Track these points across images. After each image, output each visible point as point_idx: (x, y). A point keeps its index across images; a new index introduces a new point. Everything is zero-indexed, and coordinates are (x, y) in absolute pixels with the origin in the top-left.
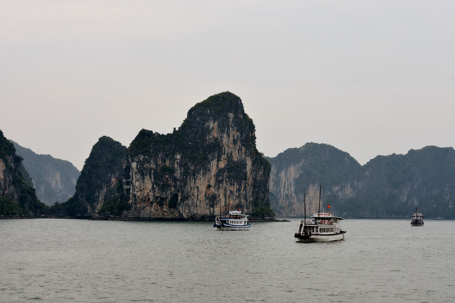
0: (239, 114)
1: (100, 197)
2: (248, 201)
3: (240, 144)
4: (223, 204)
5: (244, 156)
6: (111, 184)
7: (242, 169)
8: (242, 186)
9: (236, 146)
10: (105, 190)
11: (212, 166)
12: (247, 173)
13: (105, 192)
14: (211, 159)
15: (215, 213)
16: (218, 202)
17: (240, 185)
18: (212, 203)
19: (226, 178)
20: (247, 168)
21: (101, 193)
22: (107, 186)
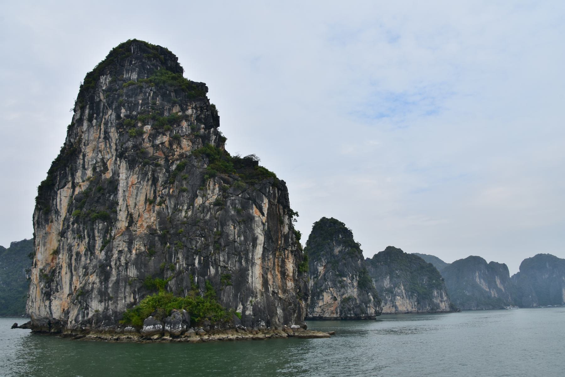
0: (125, 73)
2: (113, 278)
4: (66, 290)
6: (319, 274)
7: (108, 195)
8: (97, 238)
9: (110, 145)
11: (61, 201)
13: (312, 285)
16: (59, 286)
18: (49, 289)
19: (73, 224)
20: (119, 190)
22: (314, 278)
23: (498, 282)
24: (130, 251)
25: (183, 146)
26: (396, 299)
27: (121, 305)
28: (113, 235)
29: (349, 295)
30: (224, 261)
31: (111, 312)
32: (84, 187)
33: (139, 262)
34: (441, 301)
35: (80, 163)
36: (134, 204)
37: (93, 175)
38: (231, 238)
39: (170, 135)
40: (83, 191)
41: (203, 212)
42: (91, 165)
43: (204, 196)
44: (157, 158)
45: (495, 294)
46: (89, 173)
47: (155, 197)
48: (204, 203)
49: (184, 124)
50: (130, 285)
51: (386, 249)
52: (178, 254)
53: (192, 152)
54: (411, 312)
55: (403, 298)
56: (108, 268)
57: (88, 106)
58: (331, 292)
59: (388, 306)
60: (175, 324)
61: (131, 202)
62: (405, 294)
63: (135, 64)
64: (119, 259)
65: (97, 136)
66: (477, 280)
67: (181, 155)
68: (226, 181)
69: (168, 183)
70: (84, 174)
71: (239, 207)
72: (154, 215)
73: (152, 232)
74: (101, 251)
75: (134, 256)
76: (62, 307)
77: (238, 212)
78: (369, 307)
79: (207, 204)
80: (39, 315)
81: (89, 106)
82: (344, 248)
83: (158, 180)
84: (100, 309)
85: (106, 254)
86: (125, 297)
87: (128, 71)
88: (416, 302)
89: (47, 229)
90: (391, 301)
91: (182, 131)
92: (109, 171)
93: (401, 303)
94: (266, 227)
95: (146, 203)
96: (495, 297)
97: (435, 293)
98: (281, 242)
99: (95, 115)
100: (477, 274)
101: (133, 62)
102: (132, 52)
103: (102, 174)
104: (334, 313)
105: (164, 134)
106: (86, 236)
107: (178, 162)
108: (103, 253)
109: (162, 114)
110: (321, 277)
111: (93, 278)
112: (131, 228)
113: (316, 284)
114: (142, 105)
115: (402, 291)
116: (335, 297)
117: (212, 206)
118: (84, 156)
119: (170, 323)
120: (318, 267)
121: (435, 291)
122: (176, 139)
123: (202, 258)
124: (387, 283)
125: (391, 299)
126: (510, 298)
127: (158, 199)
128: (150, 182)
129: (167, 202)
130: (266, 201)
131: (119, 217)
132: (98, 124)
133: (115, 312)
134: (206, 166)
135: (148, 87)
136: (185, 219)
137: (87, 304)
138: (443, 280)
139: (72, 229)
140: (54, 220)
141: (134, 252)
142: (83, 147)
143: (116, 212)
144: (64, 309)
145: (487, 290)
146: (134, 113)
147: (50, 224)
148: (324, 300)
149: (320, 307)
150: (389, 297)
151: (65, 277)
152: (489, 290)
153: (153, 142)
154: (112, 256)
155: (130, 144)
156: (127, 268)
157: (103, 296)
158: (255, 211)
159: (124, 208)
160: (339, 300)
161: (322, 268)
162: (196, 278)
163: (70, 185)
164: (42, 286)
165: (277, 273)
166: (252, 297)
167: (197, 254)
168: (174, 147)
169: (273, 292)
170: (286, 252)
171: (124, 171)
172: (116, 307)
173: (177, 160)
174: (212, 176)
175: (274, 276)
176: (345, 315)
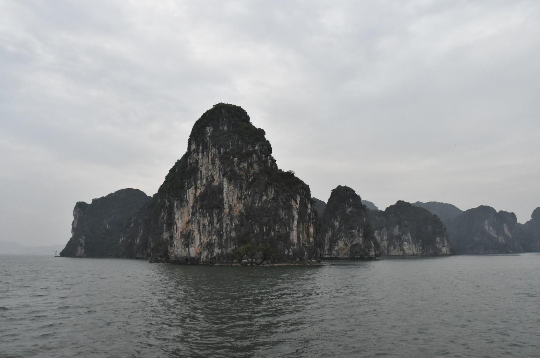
0: (220, 126)
1: (326, 240)
2: (225, 237)
3: (219, 163)
4: (198, 243)
5: (222, 178)
6: (335, 227)
7: (218, 195)
8: (214, 218)
10: (330, 233)
11: (189, 195)
12: (224, 200)
13: (331, 235)
14: (187, 187)
15: (191, 254)
16: (193, 241)
17: (211, 217)
18: (187, 242)
19: (199, 209)
20: (224, 193)
21: (326, 236)
22: (332, 230)
23: (506, 229)
24: (232, 224)
25: (254, 168)
26: (404, 244)
27: (229, 250)
28: (222, 216)
29: (356, 242)
30: (278, 229)
31: (225, 254)
32: (203, 189)
33: (236, 229)
34: (443, 246)
35: (199, 176)
36: (232, 200)
37: (207, 182)
38: (281, 216)
39: (247, 163)
40: (202, 191)
41: (266, 204)
42: (205, 177)
43: (267, 195)
44: (241, 176)
45: (502, 240)
46: (204, 181)
47: (242, 196)
48: (267, 199)
49: (255, 156)
50: (233, 240)
51: (396, 203)
52: (255, 225)
53: (259, 171)
54: (416, 255)
55: (409, 244)
56: (222, 232)
57: (201, 145)
58: (344, 240)
59: (396, 250)
60: (257, 259)
61: (231, 199)
62: (412, 240)
63: (225, 121)
64: (226, 228)
65: (207, 161)
66: (487, 227)
67: (254, 173)
68: (277, 187)
69: (248, 188)
70: (202, 182)
71: (285, 200)
72: (242, 205)
73: (241, 214)
74: (217, 224)
75: (233, 226)
76: (196, 251)
77: (284, 203)
78: (371, 251)
79: (268, 199)
80: (181, 255)
81: (202, 145)
82: (353, 209)
83: (243, 187)
84: (219, 252)
85: (220, 225)
86: (231, 247)
87: (222, 125)
88: (421, 246)
89: (182, 210)
90: (400, 245)
91: (253, 160)
92: (215, 181)
93: (408, 247)
94: (299, 211)
95: (237, 199)
96: (502, 242)
97: (438, 240)
98: (307, 218)
99: (205, 150)
100: (487, 222)
101: (224, 120)
102: (223, 113)
103: (212, 183)
104: (345, 255)
105: (244, 162)
106: (208, 216)
107: (252, 177)
108: (218, 225)
109: (242, 150)
110: (337, 230)
111: (214, 237)
112: (231, 212)
113: (333, 234)
114: (232, 145)
115: (409, 238)
116: (347, 244)
117: (271, 200)
118: (201, 172)
119: (255, 259)
120: (335, 223)
121: (438, 238)
122: (251, 165)
123: (267, 227)
124: (396, 231)
125: (399, 244)
126: (516, 244)
127: (243, 197)
128: (239, 189)
129: (248, 198)
130: (299, 197)
131: (225, 207)
132: (207, 154)
133: (227, 254)
134: (267, 179)
135: (234, 135)
136: (258, 208)
137: (212, 250)
138: (445, 229)
139: (199, 212)
140: (185, 205)
141: (233, 224)
142: (200, 167)
143: (223, 205)
144: (197, 252)
145: (495, 236)
146: (228, 150)
147: (183, 208)
148: (339, 246)
149: (336, 250)
150: (398, 243)
151: (197, 237)
152: (497, 236)
153: (239, 167)
154: (223, 226)
155: (228, 169)
156: (231, 232)
157: (220, 246)
158: (293, 203)
159: (227, 202)
160: (350, 245)
161: (338, 223)
162: (265, 237)
163: (193, 187)
164: (183, 240)
165: (305, 234)
166: (292, 246)
167: (265, 225)
168: (250, 169)
169: (303, 243)
170: (310, 223)
171: (226, 183)
172: (227, 251)
173: (252, 176)
174: (270, 184)
175: (303, 236)
176: (353, 256)
